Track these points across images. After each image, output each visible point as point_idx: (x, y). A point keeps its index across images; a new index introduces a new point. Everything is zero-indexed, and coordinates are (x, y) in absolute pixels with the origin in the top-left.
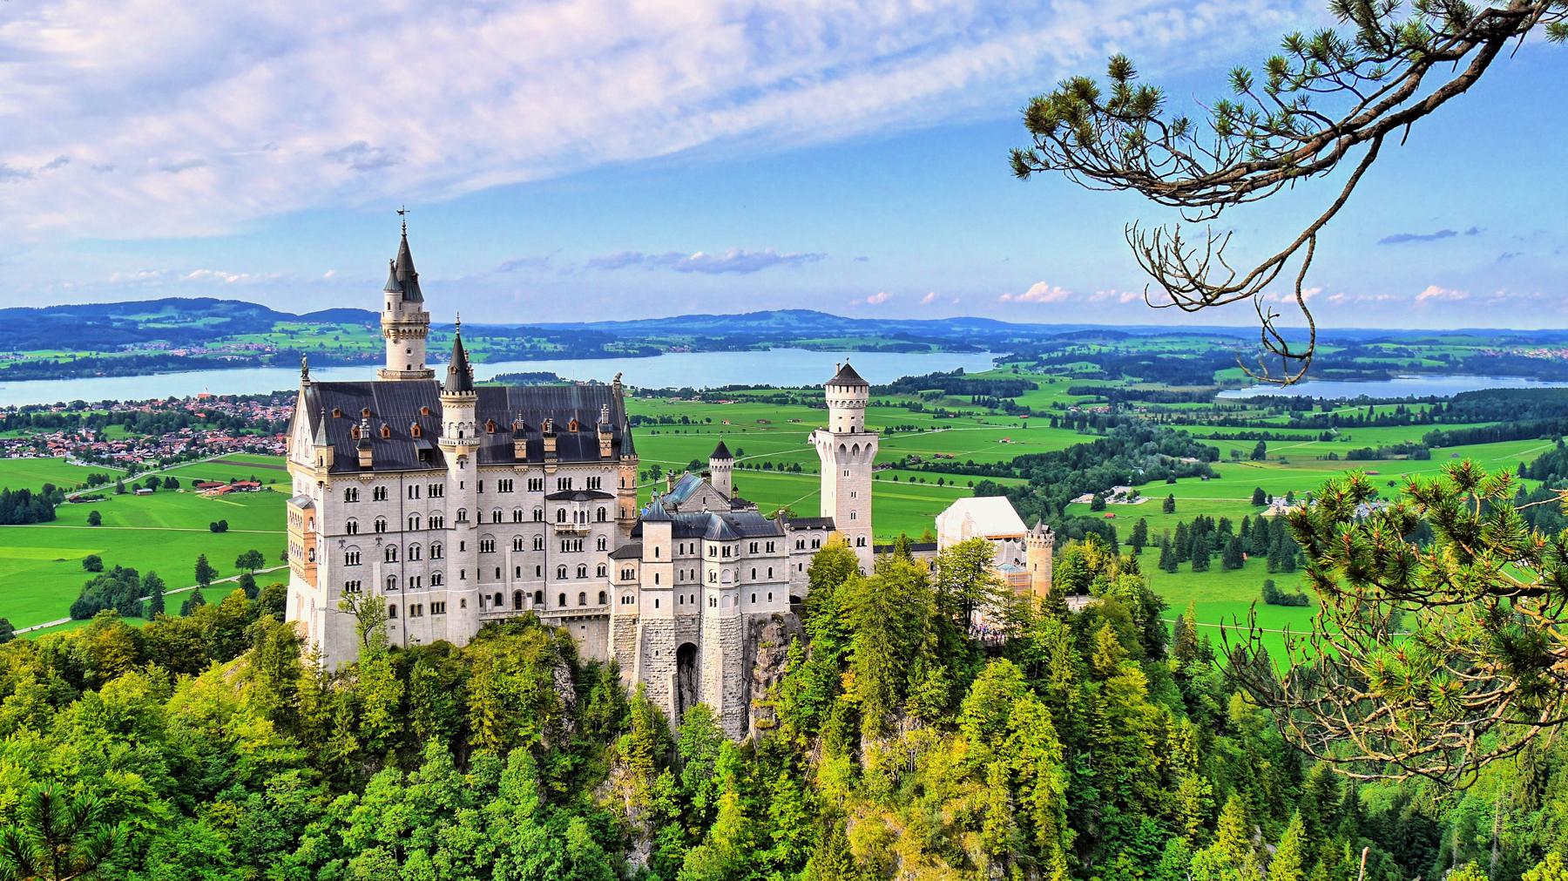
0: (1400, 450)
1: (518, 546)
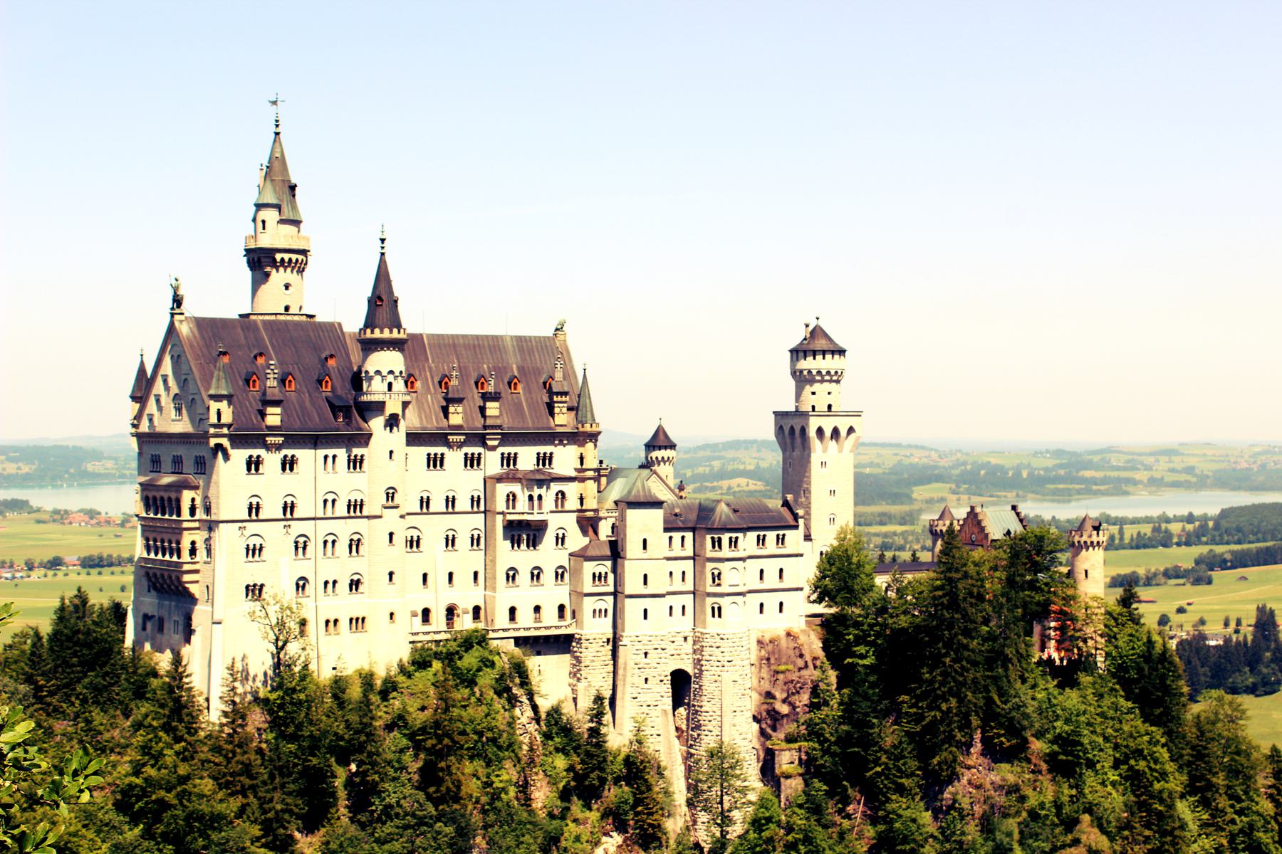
0: (1173, 574)
1: (450, 542)
